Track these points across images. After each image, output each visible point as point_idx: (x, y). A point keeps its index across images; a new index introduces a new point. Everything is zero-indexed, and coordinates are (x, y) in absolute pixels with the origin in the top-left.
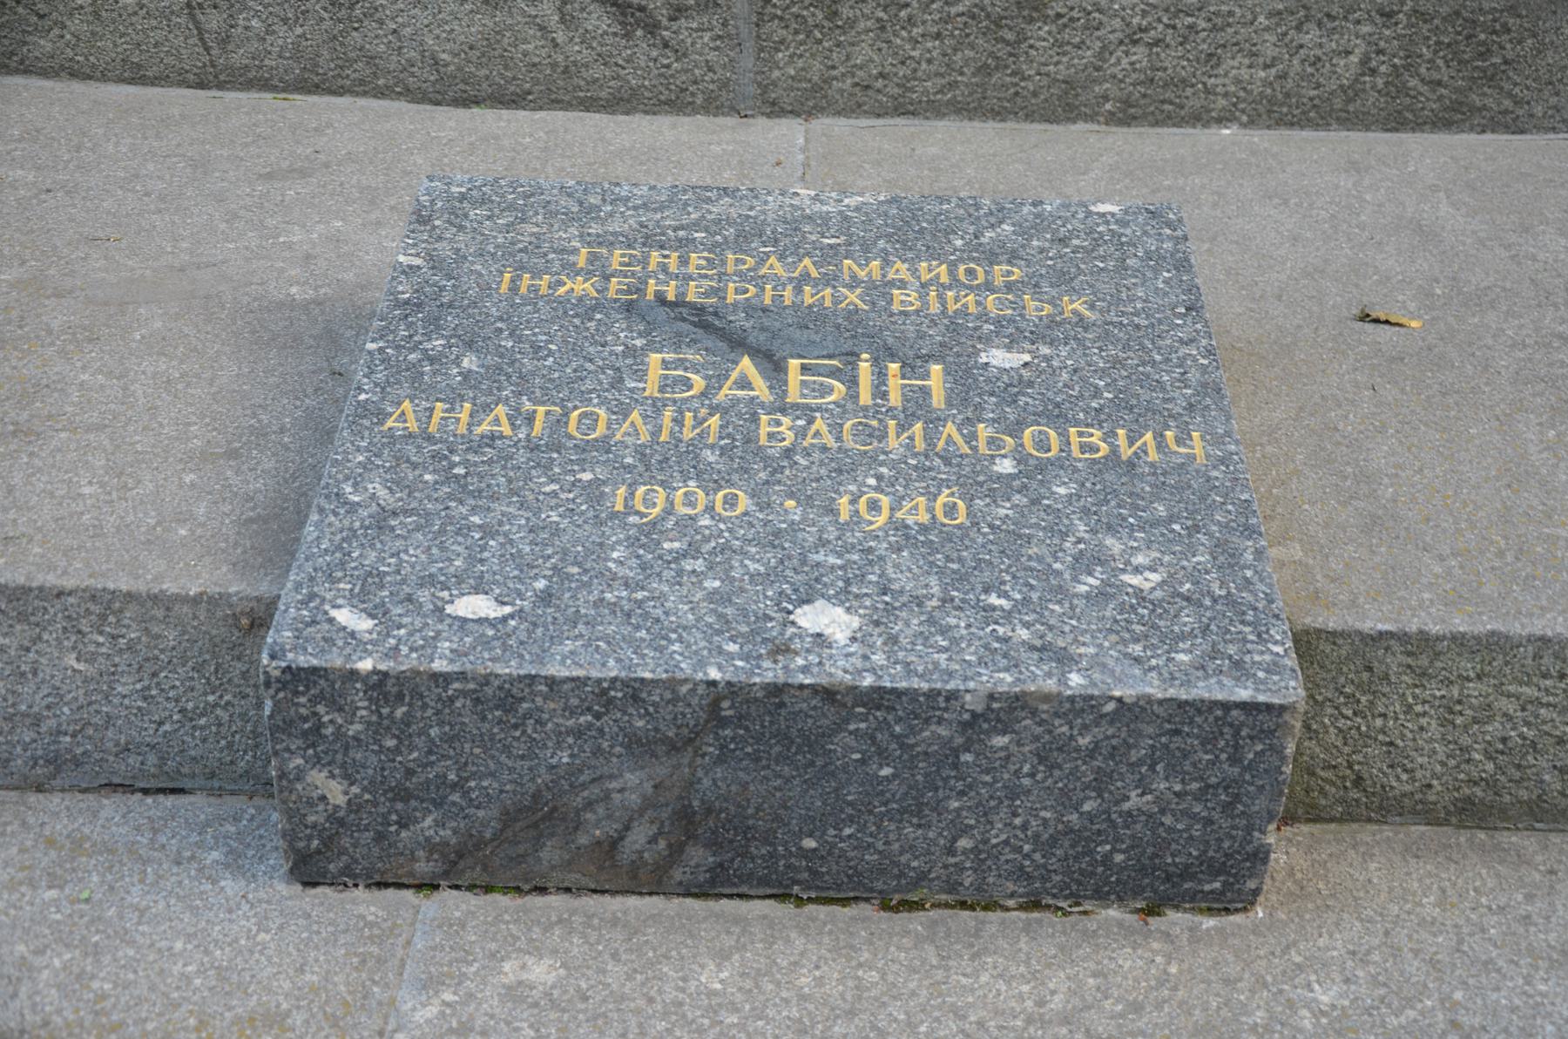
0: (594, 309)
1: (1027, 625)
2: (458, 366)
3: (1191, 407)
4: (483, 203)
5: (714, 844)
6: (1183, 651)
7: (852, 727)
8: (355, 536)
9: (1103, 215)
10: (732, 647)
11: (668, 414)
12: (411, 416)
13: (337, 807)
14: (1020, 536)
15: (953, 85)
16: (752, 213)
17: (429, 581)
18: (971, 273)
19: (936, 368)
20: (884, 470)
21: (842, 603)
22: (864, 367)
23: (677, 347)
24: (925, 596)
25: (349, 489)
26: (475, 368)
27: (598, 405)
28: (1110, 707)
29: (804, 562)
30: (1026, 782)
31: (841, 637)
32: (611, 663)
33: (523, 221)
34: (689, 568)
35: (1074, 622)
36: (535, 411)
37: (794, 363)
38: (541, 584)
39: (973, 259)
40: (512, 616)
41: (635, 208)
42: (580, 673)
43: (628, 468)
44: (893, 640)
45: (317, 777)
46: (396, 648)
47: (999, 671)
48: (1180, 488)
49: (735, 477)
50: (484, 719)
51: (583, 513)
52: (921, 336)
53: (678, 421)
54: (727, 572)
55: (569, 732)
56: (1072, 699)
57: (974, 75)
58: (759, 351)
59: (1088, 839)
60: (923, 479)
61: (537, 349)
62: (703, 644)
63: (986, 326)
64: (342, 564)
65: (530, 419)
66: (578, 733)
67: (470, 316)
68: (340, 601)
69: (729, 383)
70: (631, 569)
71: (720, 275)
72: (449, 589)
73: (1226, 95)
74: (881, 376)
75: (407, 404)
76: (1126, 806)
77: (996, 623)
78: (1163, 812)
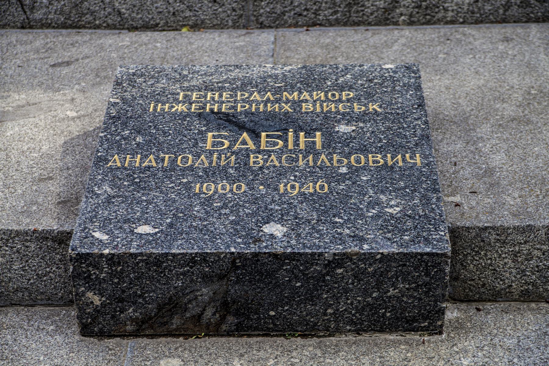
0: (186, 116)
1: (349, 228)
2: (135, 141)
3: (416, 145)
4: (142, 76)
5: (237, 314)
6: (406, 235)
7: (284, 268)
8: (100, 206)
9: (387, 69)
10: (239, 240)
11: (215, 156)
12: (118, 161)
13: (97, 306)
14: (348, 196)
15: (336, 12)
16: (248, 75)
18: (333, 95)
20: (297, 173)
21: (280, 223)
23: (218, 130)
25: (96, 189)
26: (141, 141)
27: (189, 153)
28: (379, 256)
29: (266, 209)
30: (351, 286)
31: (279, 235)
32: (195, 247)
33: (158, 82)
35: (366, 227)
36: (165, 157)
37: (263, 134)
38: (169, 221)
40: (159, 232)
41: (201, 75)
42: (185, 251)
43: (200, 177)
44: (299, 235)
45: (90, 294)
46: (117, 245)
48: (409, 176)
49: (241, 178)
50: (150, 270)
51: (184, 194)
52: (313, 121)
53: (219, 158)
55: (182, 274)
56: (364, 254)
57: (345, 7)
58: (250, 130)
59: (375, 308)
60: (311, 176)
61: (165, 133)
63: (339, 116)
64: (96, 216)
65: (163, 160)
66: (184, 274)
67: (138, 121)
68: (96, 230)
70: (202, 213)
71: (235, 100)
72: (135, 223)
73: (453, 11)
74: (297, 138)
76: (389, 294)
78: (403, 296)
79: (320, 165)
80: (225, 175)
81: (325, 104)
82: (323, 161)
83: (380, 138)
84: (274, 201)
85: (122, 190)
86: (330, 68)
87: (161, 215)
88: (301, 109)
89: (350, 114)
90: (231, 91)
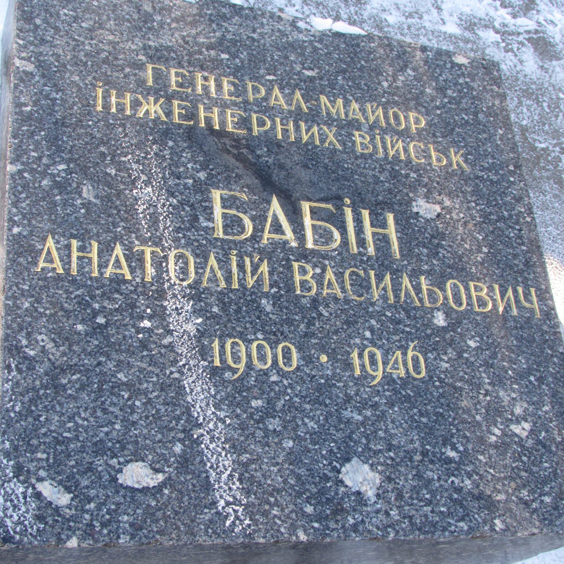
1: (469, 476)
10: (309, 509)
14: (455, 388)
16: (255, 36)
17: (100, 449)
19: (390, 218)
22: (349, 214)
25: (24, 342)
29: (340, 420)
31: (370, 494)
33: (101, 27)
34: (271, 427)
35: (492, 471)
36: (143, 252)
38: (178, 448)
39: (396, 103)
41: (177, 20)
44: (400, 496)
46: (90, 525)
47: (459, 521)
52: (377, 181)
53: (241, 267)
62: (291, 507)
65: (141, 260)
68: (42, 473)
74: (358, 221)
77: (453, 475)
79: (405, 301)
80: (259, 318)
82: (407, 294)
84: (348, 399)
85: (75, 348)
86: (380, 46)
87: (161, 429)
90: (236, 77)
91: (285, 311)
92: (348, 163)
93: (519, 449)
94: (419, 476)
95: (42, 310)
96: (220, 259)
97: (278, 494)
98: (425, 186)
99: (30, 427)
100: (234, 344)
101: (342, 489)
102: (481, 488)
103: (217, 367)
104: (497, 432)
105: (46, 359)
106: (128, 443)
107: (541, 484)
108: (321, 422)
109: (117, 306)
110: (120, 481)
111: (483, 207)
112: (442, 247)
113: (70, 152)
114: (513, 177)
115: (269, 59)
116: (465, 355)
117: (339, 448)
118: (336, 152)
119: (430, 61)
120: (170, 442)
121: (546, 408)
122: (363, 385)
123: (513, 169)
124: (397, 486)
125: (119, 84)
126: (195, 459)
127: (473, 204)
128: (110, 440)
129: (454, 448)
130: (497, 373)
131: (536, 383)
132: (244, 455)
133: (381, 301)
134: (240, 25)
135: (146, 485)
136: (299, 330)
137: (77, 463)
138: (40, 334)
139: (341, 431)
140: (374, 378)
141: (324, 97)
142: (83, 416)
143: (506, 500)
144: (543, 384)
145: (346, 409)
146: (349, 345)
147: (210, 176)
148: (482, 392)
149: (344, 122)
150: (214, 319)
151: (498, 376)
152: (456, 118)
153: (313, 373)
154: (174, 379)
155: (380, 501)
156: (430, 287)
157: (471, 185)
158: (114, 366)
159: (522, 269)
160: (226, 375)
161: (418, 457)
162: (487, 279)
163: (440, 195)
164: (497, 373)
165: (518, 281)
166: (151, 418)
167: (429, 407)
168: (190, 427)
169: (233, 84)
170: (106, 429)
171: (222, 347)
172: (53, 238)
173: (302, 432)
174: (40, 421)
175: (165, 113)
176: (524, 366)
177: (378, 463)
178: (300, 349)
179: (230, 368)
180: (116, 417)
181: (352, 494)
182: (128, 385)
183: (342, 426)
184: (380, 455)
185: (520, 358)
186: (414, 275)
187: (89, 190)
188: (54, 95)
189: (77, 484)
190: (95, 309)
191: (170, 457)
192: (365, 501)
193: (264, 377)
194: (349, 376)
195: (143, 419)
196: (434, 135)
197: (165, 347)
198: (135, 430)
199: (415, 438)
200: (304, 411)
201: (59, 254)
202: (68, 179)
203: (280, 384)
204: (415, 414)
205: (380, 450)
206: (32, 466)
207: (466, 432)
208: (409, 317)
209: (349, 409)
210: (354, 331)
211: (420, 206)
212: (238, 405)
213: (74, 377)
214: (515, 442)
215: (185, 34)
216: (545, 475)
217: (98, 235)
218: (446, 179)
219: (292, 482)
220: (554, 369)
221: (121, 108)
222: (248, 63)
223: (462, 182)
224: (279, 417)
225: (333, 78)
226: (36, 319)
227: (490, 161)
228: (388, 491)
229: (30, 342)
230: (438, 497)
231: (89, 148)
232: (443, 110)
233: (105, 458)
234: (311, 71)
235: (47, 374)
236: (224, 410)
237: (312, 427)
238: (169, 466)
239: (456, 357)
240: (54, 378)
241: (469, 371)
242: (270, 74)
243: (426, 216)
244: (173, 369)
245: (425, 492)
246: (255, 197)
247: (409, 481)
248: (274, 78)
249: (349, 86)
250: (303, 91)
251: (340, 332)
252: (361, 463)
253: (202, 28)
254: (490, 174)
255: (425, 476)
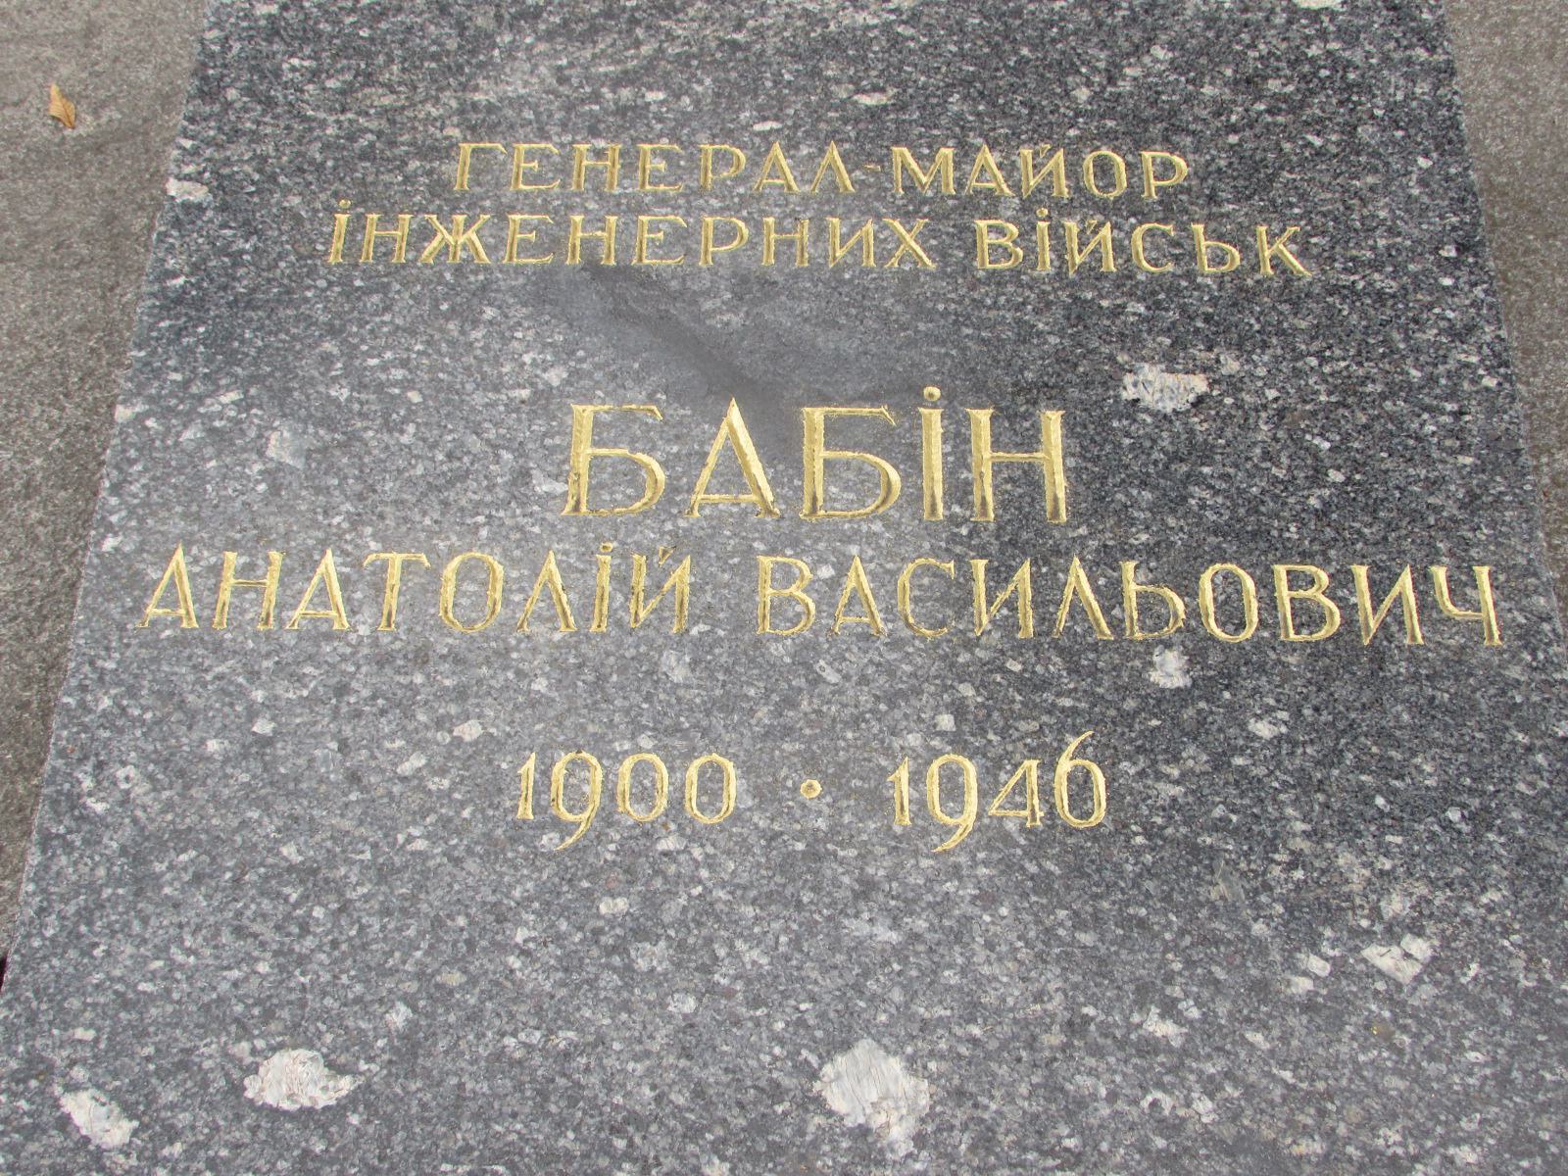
1: (1211, 1087)
3: (1471, 502)
4: (305, 40)
14: (1195, 850)
16: (739, 37)
17: (214, 1017)
18: (1103, 168)
19: (1052, 422)
22: (934, 421)
24: (1039, 1021)
25: (88, 783)
26: (289, 460)
31: (899, 1134)
33: (369, 79)
35: (1287, 1075)
36: (384, 567)
38: (399, 1016)
39: (1109, 137)
52: (1026, 334)
53: (621, 580)
54: (705, 970)
60: (1031, 710)
64: (81, 975)
68: (79, 1073)
69: (706, 474)
70: (547, 970)
72: (251, 1038)
74: (958, 439)
75: (179, 556)
77: (1160, 1085)
79: (1067, 629)
80: (648, 698)
81: (1072, 225)
82: (1078, 611)
83: (1315, 454)
84: (866, 889)
88: (971, 250)
89: (1179, 291)
90: (674, 138)
91: (721, 677)
92: (947, 301)
93: (1387, 1014)
94: (1053, 1089)
95: (137, 712)
96: (570, 565)
97: (637, 1129)
98: (1167, 332)
99: (71, 970)
100: (574, 766)
101: (819, 1120)
102: (1246, 1122)
103: (524, 821)
104: (1318, 966)
105: (127, 821)
106: (281, 1006)
107: (1448, 1110)
108: (781, 949)
109: (305, 693)
110: (249, 1094)
111: (1343, 364)
112: (1202, 481)
113: (255, 362)
114: (1451, 275)
115: (769, 84)
116: (1239, 761)
117: (822, 1016)
118: (918, 277)
119: (1225, 16)
120: (381, 1001)
121: (1491, 896)
122: (916, 853)
123: (1453, 254)
124: (979, 1113)
125: (389, 198)
126: (435, 1044)
127: (1314, 362)
128: (240, 999)
129: (1169, 1010)
130: (1337, 806)
131: (1465, 828)
132: (561, 1034)
133: (996, 635)
134: (706, 19)
135: (307, 1103)
136: (753, 722)
137: (158, 1050)
138: (124, 764)
139: (836, 973)
140: (949, 831)
141: (905, 150)
142: (188, 944)
143: (1327, 1156)
144: (1489, 828)
145: (857, 916)
146: (888, 752)
147: (575, 373)
148: (1282, 857)
149: (951, 202)
150: (533, 707)
151: (1341, 812)
152: (1287, 146)
153: (776, 827)
154: (413, 853)
155: (924, 1154)
156: (1151, 588)
157: (1311, 311)
158: (279, 831)
159: (1452, 519)
160: (545, 839)
161: (1054, 1038)
162: (1332, 553)
163: (1210, 349)
164: (1337, 806)
165: (1437, 552)
166: (344, 947)
167: (1106, 905)
168: (436, 966)
169: (666, 155)
170: (235, 974)
171: (545, 772)
172: (186, 553)
173: (724, 976)
174: (93, 957)
175: (486, 246)
176: (1431, 782)
177: (932, 1054)
178: (747, 769)
179: (557, 824)
180: (263, 944)
181: (843, 1134)
182: (305, 873)
183: (840, 958)
184: (940, 1032)
185: (1418, 760)
186: (1104, 562)
187: (282, 440)
188: (241, 244)
189: (151, 1099)
190: (254, 702)
191: (376, 1038)
192: (881, 1151)
193: (642, 841)
194: (877, 831)
195: (327, 948)
196: (1212, 199)
197: (404, 779)
198: (303, 974)
199: (1052, 987)
200: (736, 922)
201: (194, 587)
202: (241, 422)
203: (682, 858)
204: (1061, 924)
205: (941, 1018)
206: (59, 1057)
207: (1215, 969)
208: (1074, 670)
209: (866, 916)
210: (906, 716)
211: (1146, 384)
212: (565, 911)
213: (184, 857)
214: (1377, 992)
215: (564, 62)
216: (1466, 1086)
217: (287, 536)
218: (1235, 304)
219: (681, 1101)
220: (1532, 785)
221: (384, 250)
222: (713, 102)
223: (1285, 308)
224: (669, 937)
225: (934, 101)
226: (121, 731)
227: (1382, 243)
228: (952, 1128)
229: (99, 783)
230: (1104, 1146)
231: (298, 347)
232: (1248, 133)
233: (223, 1039)
234: (877, 96)
235: (123, 851)
236: (526, 923)
237: (754, 963)
238: (370, 1059)
239: (1207, 768)
240: (139, 860)
241: (1246, 801)
242: (765, 119)
243: (1160, 406)
244: (416, 832)
245: (1064, 1130)
246: (682, 412)
247: (1020, 1102)
248: (775, 125)
249: (978, 115)
250: (847, 146)
251: (867, 721)
252: (882, 1052)
253: (609, 40)
254: (1376, 276)
255: (1070, 1087)
